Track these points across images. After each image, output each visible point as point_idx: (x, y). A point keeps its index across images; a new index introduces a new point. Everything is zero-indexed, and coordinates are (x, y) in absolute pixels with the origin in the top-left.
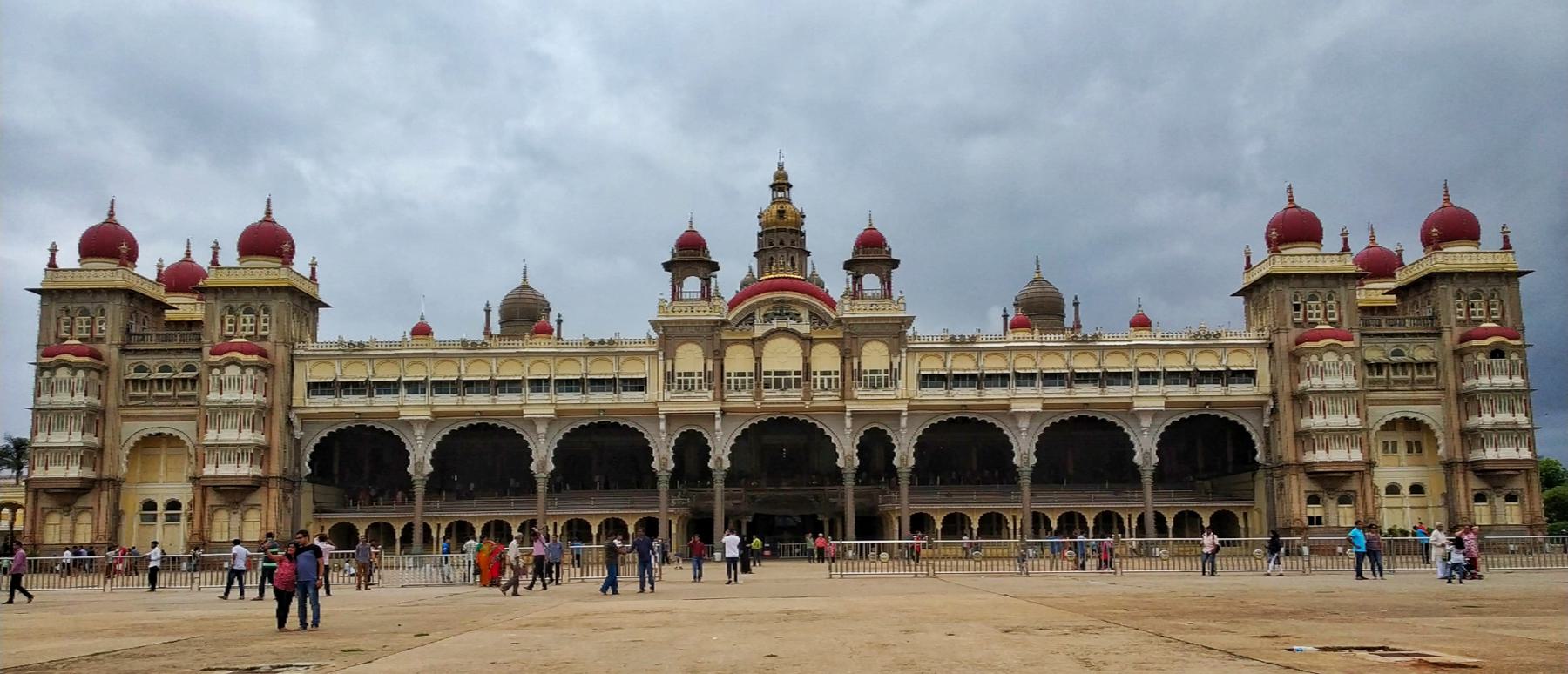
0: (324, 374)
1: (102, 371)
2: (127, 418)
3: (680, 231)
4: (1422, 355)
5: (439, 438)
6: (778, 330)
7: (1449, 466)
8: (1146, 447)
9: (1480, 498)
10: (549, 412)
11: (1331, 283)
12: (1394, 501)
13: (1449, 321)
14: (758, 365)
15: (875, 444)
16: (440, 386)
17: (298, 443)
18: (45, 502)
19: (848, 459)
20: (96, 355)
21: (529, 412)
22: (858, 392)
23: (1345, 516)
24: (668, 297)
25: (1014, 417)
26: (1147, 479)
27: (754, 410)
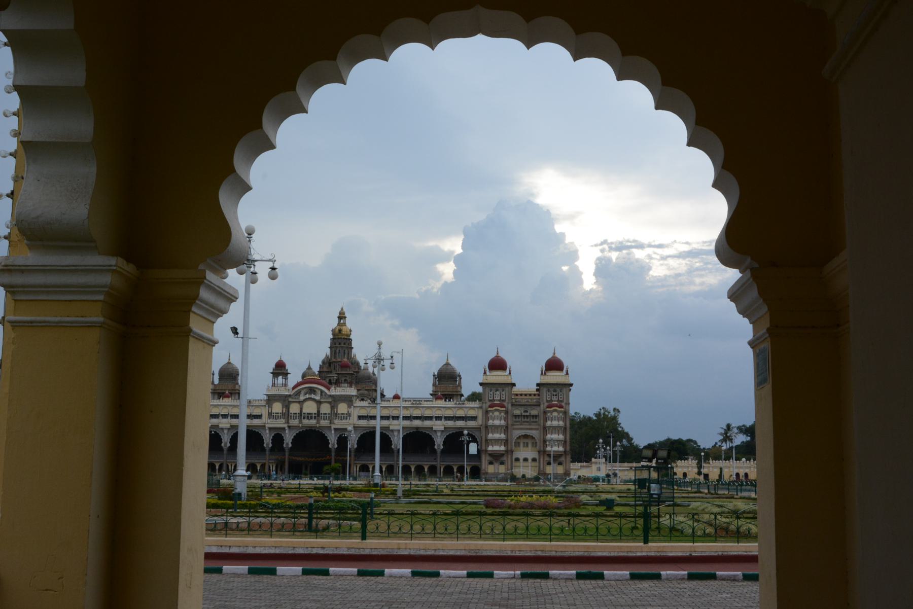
3: (277, 360)
4: (534, 412)
7: (539, 452)
10: (228, 426)
12: (525, 464)
15: (342, 441)
19: (333, 445)
21: (221, 426)
22: (336, 421)
23: (502, 469)
24: (271, 385)
25: (392, 431)
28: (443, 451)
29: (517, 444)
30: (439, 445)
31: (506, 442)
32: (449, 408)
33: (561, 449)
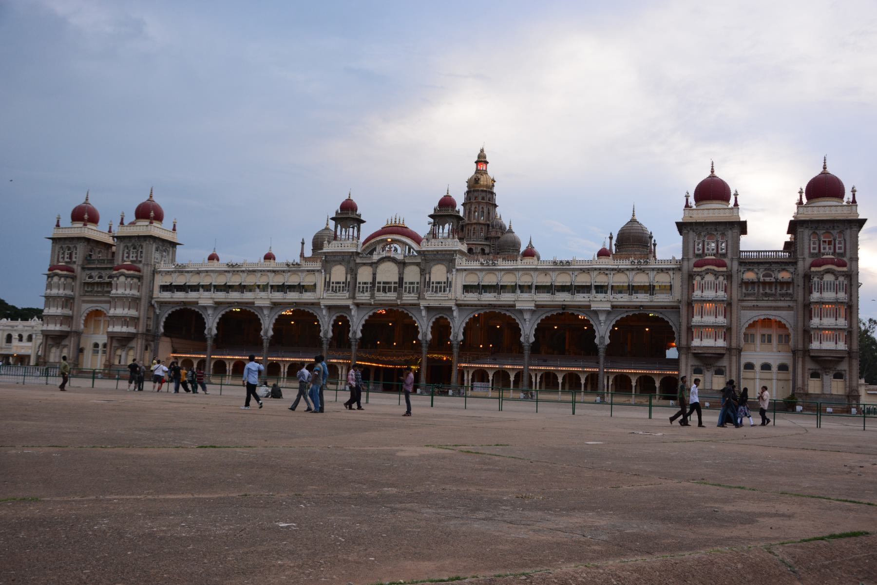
0: (167, 280)
1: (74, 278)
2: (84, 302)
4: (784, 276)
5: (220, 316)
6: (386, 257)
7: (794, 352)
8: (602, 333)
9: (815, 375)
11: (721, 228)
12: (766, 375)
13: (803, 254)
14: (374, 278)
16: (218, 288)
17: (158, 316)
18: (50, 342)
20: (72, 271)
21: (258, 303)
22: (428, 295)
26: (602, 354)
27: (371, 304)
28: (610, 349)
29: (749, 338)
30: (602, 338)
31: (727, 331)
32: (619, 271)
33: (842, 346)
